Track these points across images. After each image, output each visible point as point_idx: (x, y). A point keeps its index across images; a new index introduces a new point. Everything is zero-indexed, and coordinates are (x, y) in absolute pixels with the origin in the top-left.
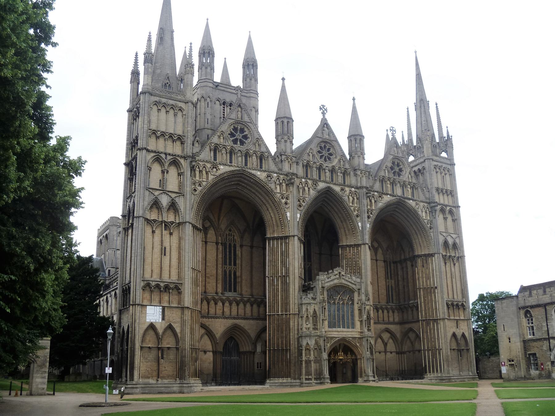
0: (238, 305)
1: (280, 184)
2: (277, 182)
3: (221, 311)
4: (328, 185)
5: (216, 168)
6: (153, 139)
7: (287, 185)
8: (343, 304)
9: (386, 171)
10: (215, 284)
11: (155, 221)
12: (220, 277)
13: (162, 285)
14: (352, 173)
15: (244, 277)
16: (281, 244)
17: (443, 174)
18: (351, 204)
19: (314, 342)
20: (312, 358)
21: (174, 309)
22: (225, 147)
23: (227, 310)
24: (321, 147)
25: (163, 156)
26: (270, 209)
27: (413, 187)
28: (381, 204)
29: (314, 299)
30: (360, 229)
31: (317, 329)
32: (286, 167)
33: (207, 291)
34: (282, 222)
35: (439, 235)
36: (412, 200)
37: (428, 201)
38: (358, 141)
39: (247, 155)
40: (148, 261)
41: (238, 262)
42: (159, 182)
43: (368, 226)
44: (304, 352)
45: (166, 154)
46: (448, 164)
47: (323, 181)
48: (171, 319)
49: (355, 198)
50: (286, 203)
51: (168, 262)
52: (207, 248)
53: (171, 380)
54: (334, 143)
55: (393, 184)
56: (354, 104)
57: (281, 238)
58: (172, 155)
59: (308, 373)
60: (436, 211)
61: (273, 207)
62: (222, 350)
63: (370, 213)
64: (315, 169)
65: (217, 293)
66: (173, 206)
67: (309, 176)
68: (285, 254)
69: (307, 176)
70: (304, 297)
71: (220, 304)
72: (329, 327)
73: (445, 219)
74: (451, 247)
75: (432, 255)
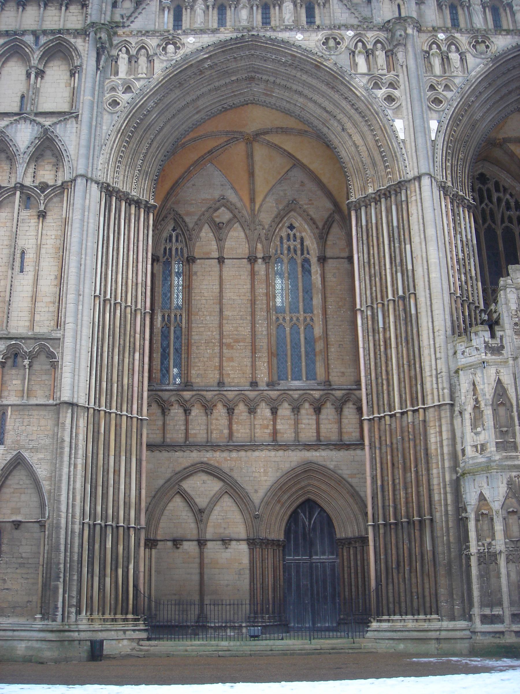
0: (318, 411)
1: (369, 54)
3: (269, 430)
5: (174, 44)
7: (390, 54)
10: (247, 362)
12: (262, 343)
15: (332, 339)
16: (389, 211)
19: (503, 489)
20: (500, 543)
23: (285, 428)
25: (29, 39)
26: (349, 125)
33: (226, 380)
34: (385, 150)
41: (317, 301)
42: (18, 99)
44: (472, 525)
50: (390, 99)
51: (29, 288)
52: (225, 274)
53: (22, 621)
57: (386, 194)
59: (491, 599)
61: (357, 117)
62: (282, 537)
65: (254, 384)
68: (400, 235)
70: (460, 348)
71: (264, 411)
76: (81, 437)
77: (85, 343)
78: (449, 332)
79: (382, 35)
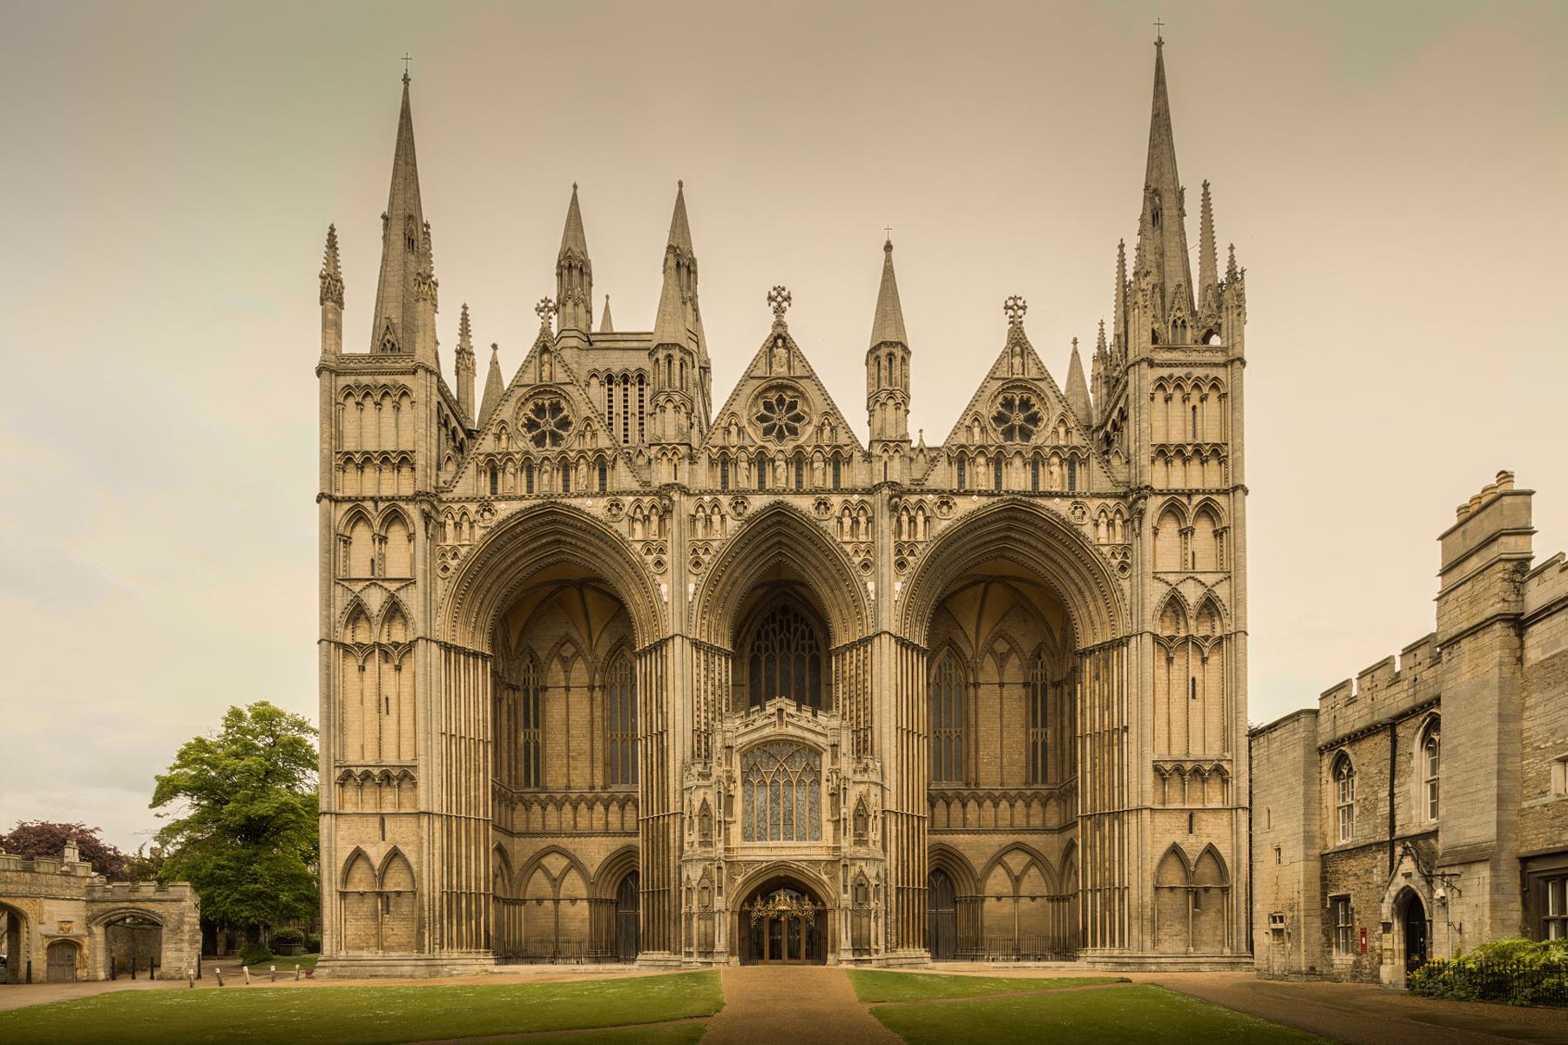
2: (638, 516)
6: (352, 472)
7: (662, 519)
8: (789, 783)
9: (977, 430)
11: (360, 645)
13: (376, 772)
14: (857, 456)
18: (847, 538)
19: (700, 873)
20: (695, 909)
21: (404, 818)
22: (508, 456)
24: (768, 406)
25: (369, 505)
27: (1073, 460)
28: (945, 524)
30: (873, 597)
31: (710, 844)
35: (1148, 580)
36: (1062, 496)
37: (1121, 490)
38: (884, 363)
39: (565, 466)
40: (353, 725)
43: (898, 586)
45: (375, 500)
46: (1216, 365)
47: (769, 492)
48: (398, 838)
49: (862, 520)
50: (659, 563)
60: (1141, 513)
64: (745, 465)
66: (394, 610)
67: (731, 486)
73: (1185, 533)
74: (1192, 612)
76: (437, 835)
77: (436, 769)
78: (689, 760)
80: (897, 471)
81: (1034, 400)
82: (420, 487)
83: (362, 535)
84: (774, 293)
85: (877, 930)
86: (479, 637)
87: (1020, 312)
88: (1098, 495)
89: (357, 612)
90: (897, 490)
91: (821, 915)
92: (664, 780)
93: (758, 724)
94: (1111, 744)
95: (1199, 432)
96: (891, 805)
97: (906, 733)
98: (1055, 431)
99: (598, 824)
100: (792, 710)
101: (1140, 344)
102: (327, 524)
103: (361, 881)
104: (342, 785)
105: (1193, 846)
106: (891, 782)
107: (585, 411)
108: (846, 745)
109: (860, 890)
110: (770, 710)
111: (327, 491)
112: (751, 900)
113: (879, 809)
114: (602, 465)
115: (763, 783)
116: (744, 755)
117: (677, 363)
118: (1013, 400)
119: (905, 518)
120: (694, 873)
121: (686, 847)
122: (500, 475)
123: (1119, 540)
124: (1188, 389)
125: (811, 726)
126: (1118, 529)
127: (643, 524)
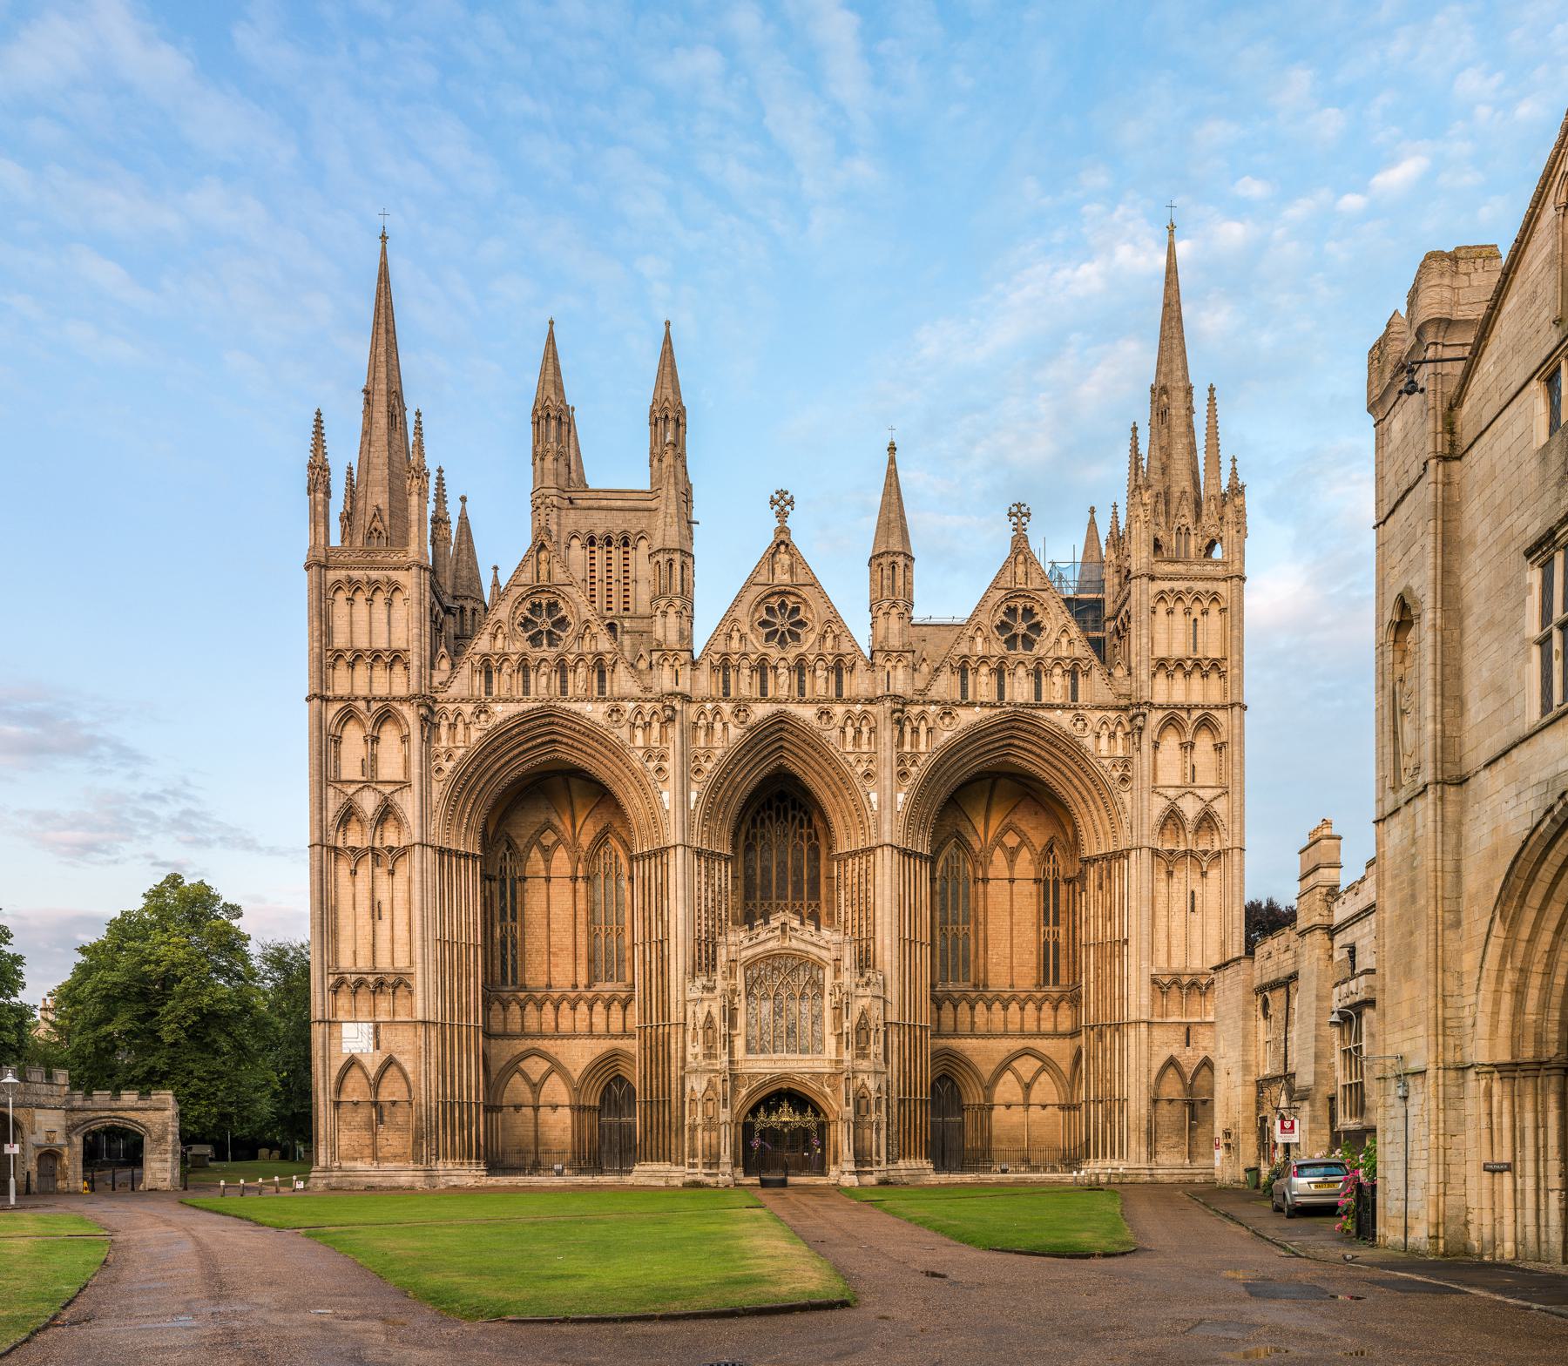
2: (639, 722)
4: (783, 707)
9: (979, 640)
11: (353, 849)
13: (371, 979)
17: (1197, 608)
18: (849, 748)
19: (705, 1085)
20: (699, 1120)
22: (504, 657)
24: (770, 610)
25: (361, 705)
28: (947, 735)
29: (711, 989)
30: (875, 807)
32: (664, 680)
36: (1063, 707)
39: (562, 667)
43: (901, 797)
50: (660, 770)
54: (805, 592)
55: (999, 672)
56: (892, 461)
58: (381, 700)
60: (1140, 729)
63: (908, 763)
64: (747, 672)
66: (386, 812)
69: (726, 694)
72: (749, 1050)
74: (1190, 827)
75: (1122, 855)
78: (689, 969)
79: (659, 706)
80: (901, 683)
81: (1037, 609)
82: (414, 689)
83: (353, 737)
84: (777, 497)
85: (877, 1141)
86: (471, 838)
87: (1024, 519)
88: (1098, 708)
89: (348, 814)
90: (902, 702)
91: (823, 1128)
92: (664, 989)
93: (762, 937)
94: (1112, 955)
95: (1199, 646)
96: (893, 1016)
97: (907, 943)
98: (1058, 641)
99: (582, 1026)
100: (796, 924)
101: (1140, 557)
102: (319, 723)
103: (356, 1089)
104: (335, 992)
105: (1190, 1058)
106: (893, 994)
107: (586, 612)
108: (847, 961)
109: (863, 1102)
110: (774, 924)
111: (317, 691)
112: (754, 1111)
113: (881, 1022)
114: (600, 668)
115: (764, 998)
116: (747, 968)
117: (677, 566)
118: (1015, 610)
119: (908, 729)
120: (697, 1085)
121: (689, 1058)
122: (495, 675)
123: (1120, 753)
124: (1188, 603)
125: (814, 939)
126: (1120, 741)
127: (644, 730)
